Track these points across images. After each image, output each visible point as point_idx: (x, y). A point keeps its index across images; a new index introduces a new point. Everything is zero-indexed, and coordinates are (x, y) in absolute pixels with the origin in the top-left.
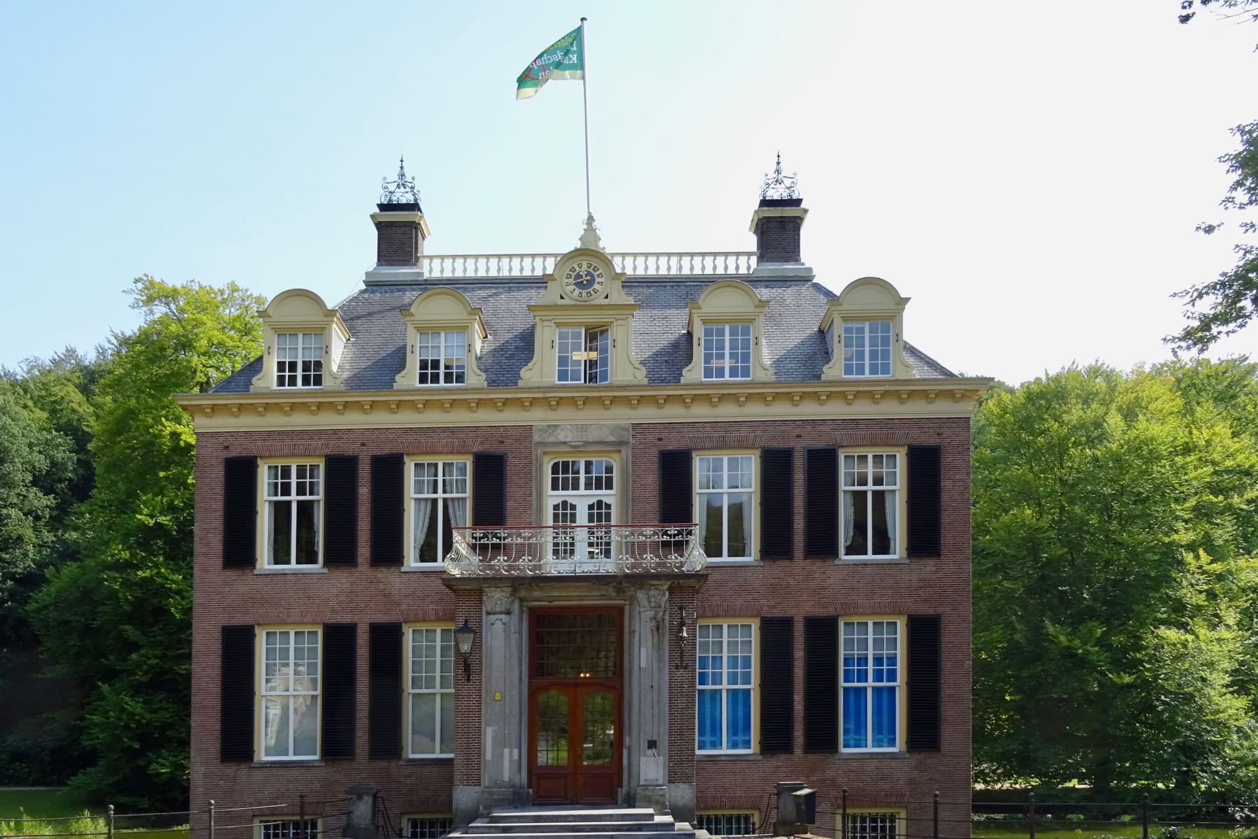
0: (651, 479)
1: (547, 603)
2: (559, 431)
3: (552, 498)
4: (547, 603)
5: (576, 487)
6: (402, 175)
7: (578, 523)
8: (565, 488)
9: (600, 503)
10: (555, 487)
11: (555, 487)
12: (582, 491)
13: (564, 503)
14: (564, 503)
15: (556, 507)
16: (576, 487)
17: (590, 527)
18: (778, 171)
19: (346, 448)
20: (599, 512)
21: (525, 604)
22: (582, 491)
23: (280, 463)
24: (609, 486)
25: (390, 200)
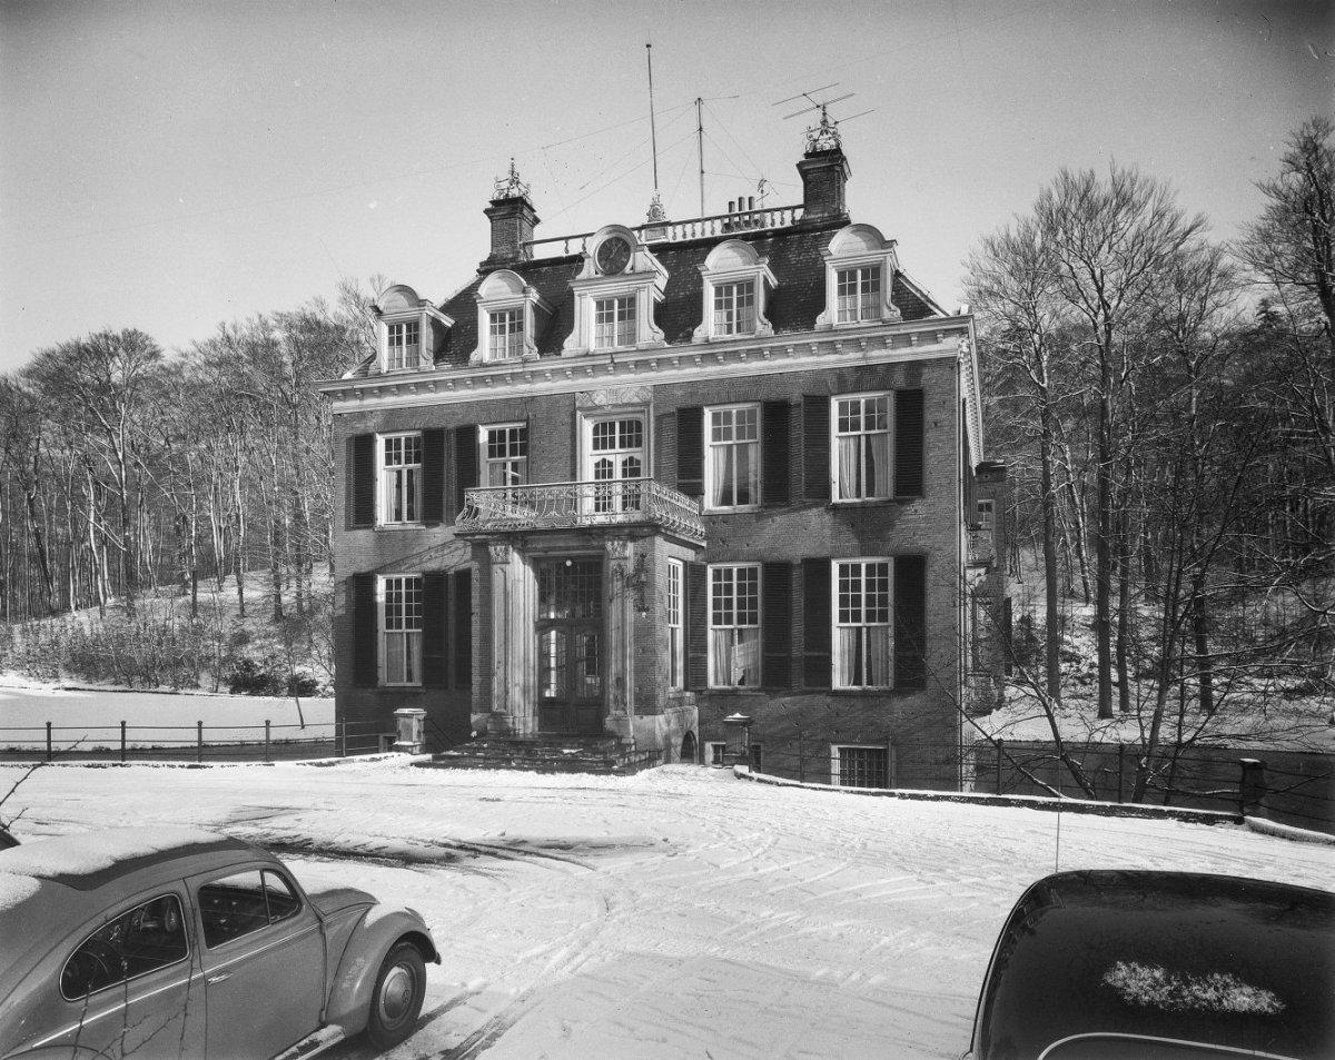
0: (671, 436)
1: (542, 554)
2: (595, 395)
4: (542, 554)
5: (613, 446)
6: (824, 122)
7: (614, 479)
8: (604, 447)
9: (631, 459)
11: (596, 447)
12: (617, 449)
14: (604, 460)
16: (613, 446)
17: (624, 482)
18: (824, 122)
20: (632, 468)
21: (527, 555)
22: (617, 449)
24: (639, 444)
25: (815, 148)
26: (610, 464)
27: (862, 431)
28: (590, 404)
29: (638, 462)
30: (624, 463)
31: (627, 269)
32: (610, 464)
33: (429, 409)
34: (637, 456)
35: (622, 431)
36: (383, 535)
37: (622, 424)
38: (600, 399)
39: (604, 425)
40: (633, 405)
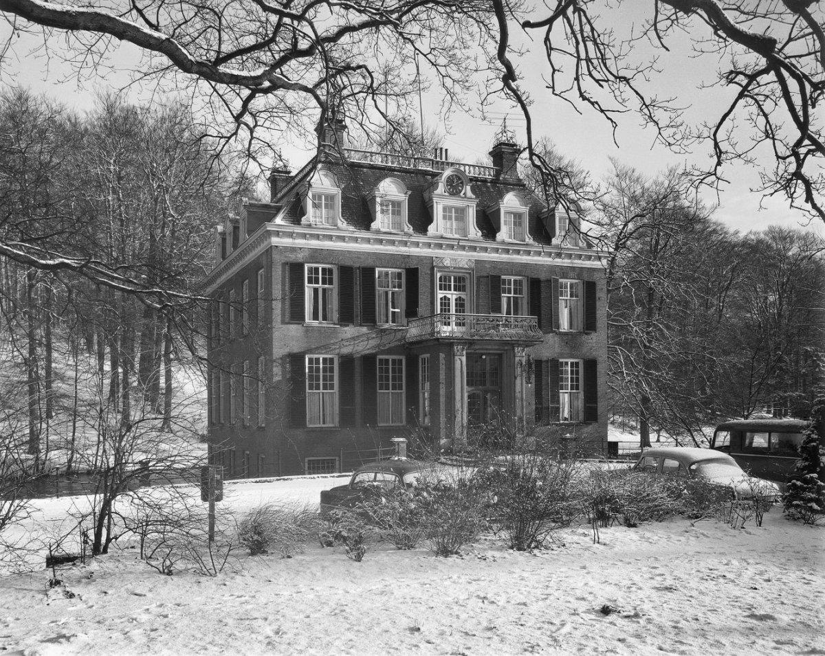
3: (440, 294)
5: (450, 290)
9: (460, 297)
10: (441, 289)
12: (452, 292)
13: (445, 297)
14: (445, 297)
15: (441, 299)
19: (348, 263)
23: (314, 265)
24: (464, 291)
26: (449, 299)
27: (569, 298)
28: (441, 265)
29: (464, 300)
30: (456, 300)
31: (462, 194)
32: (449, 299)
33: (342, 253)
34: (463, 297)
35: (455, 281)
36: (308, 329)
37: (455, 278)
38: (447, 263)
39: (445, 277)
40: (465, 269)
